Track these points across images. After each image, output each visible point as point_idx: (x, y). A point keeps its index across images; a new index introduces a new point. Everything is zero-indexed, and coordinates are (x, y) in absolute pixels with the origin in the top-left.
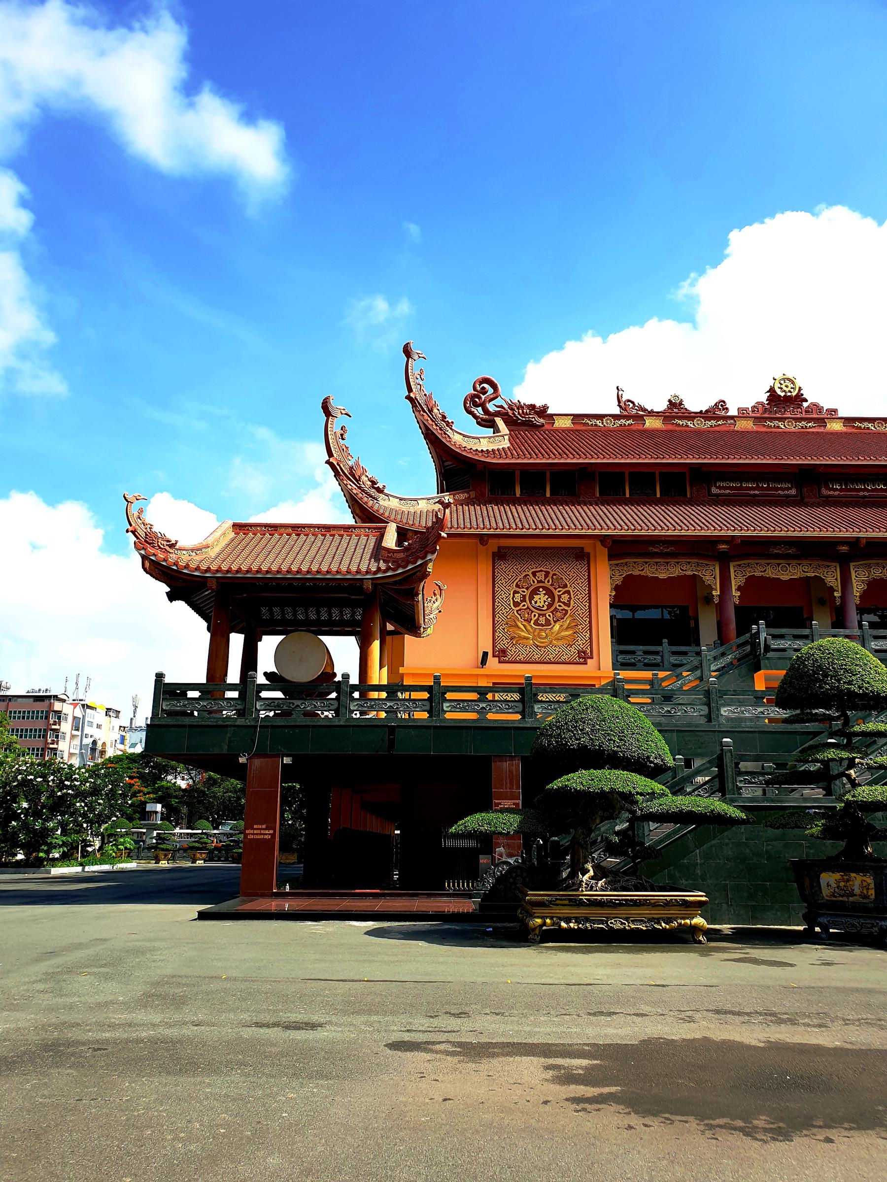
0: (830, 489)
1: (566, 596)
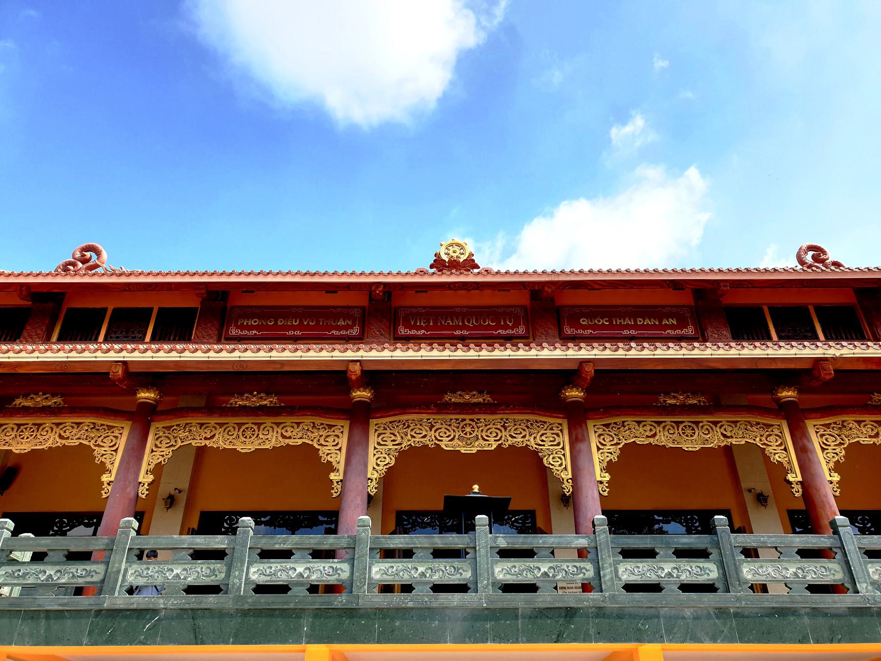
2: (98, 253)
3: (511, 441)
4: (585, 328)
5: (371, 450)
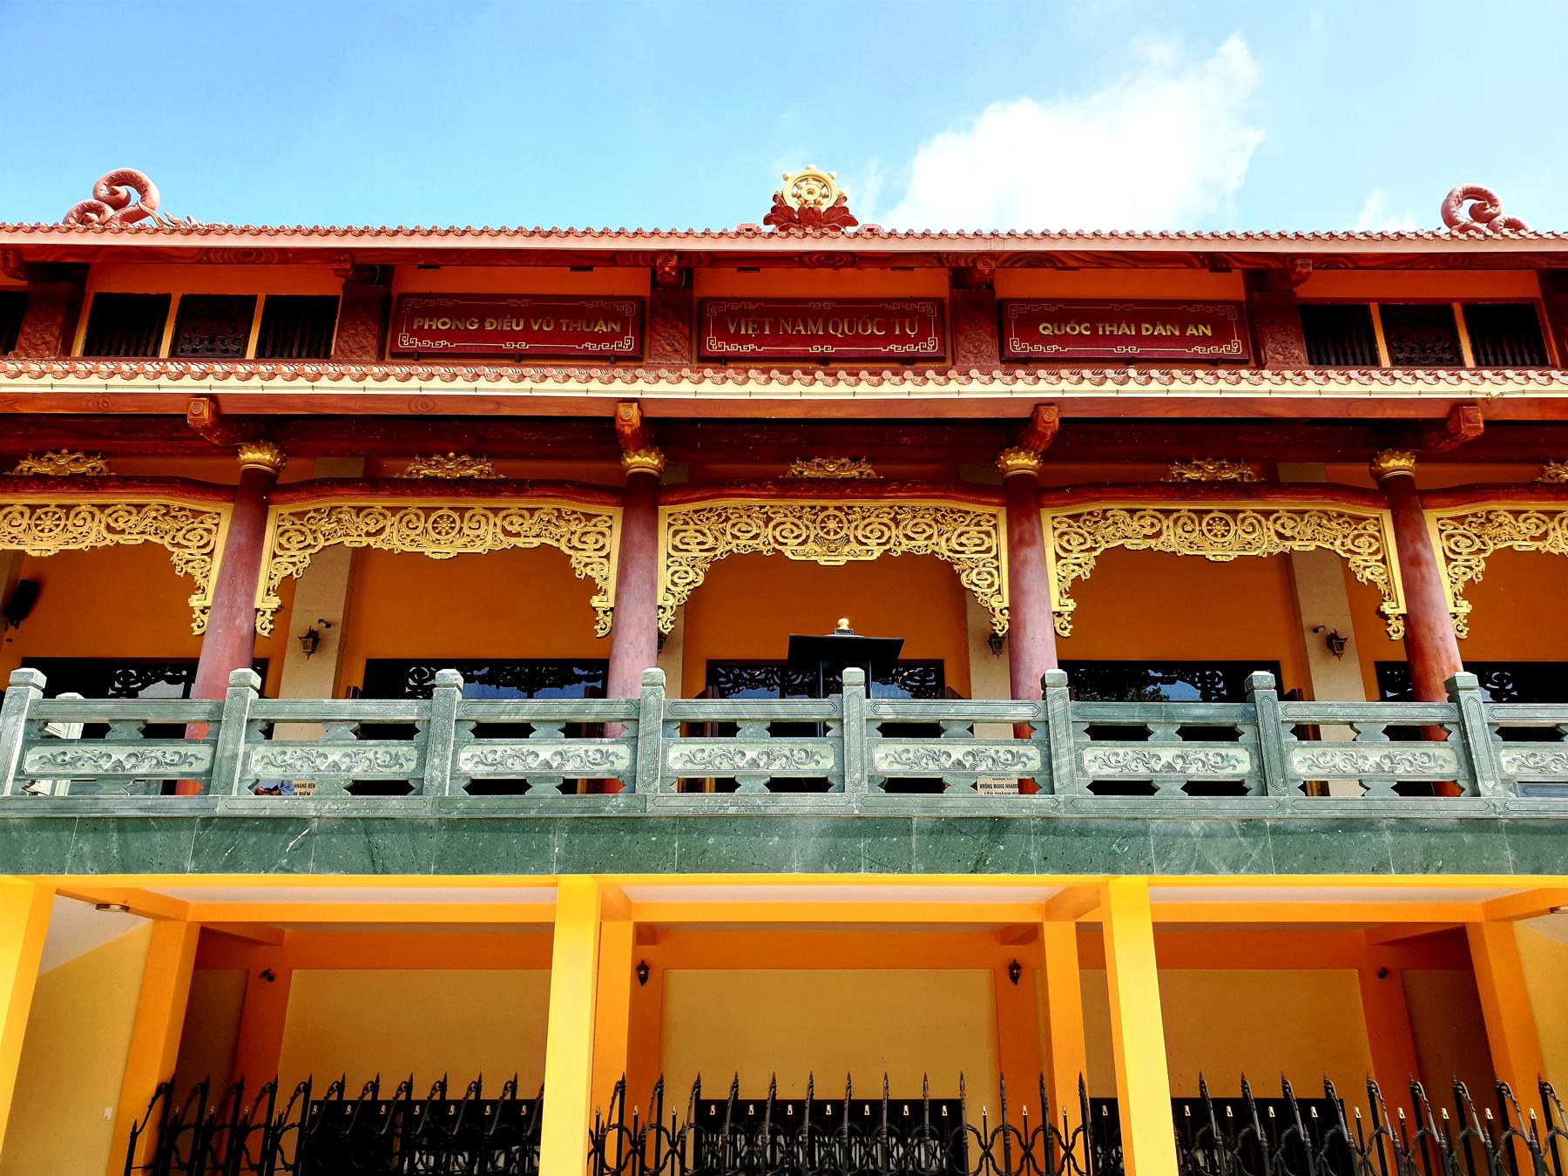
2: (142, 188)
3: (906, 545)
4: (1047, 341)
5: (662, 559)
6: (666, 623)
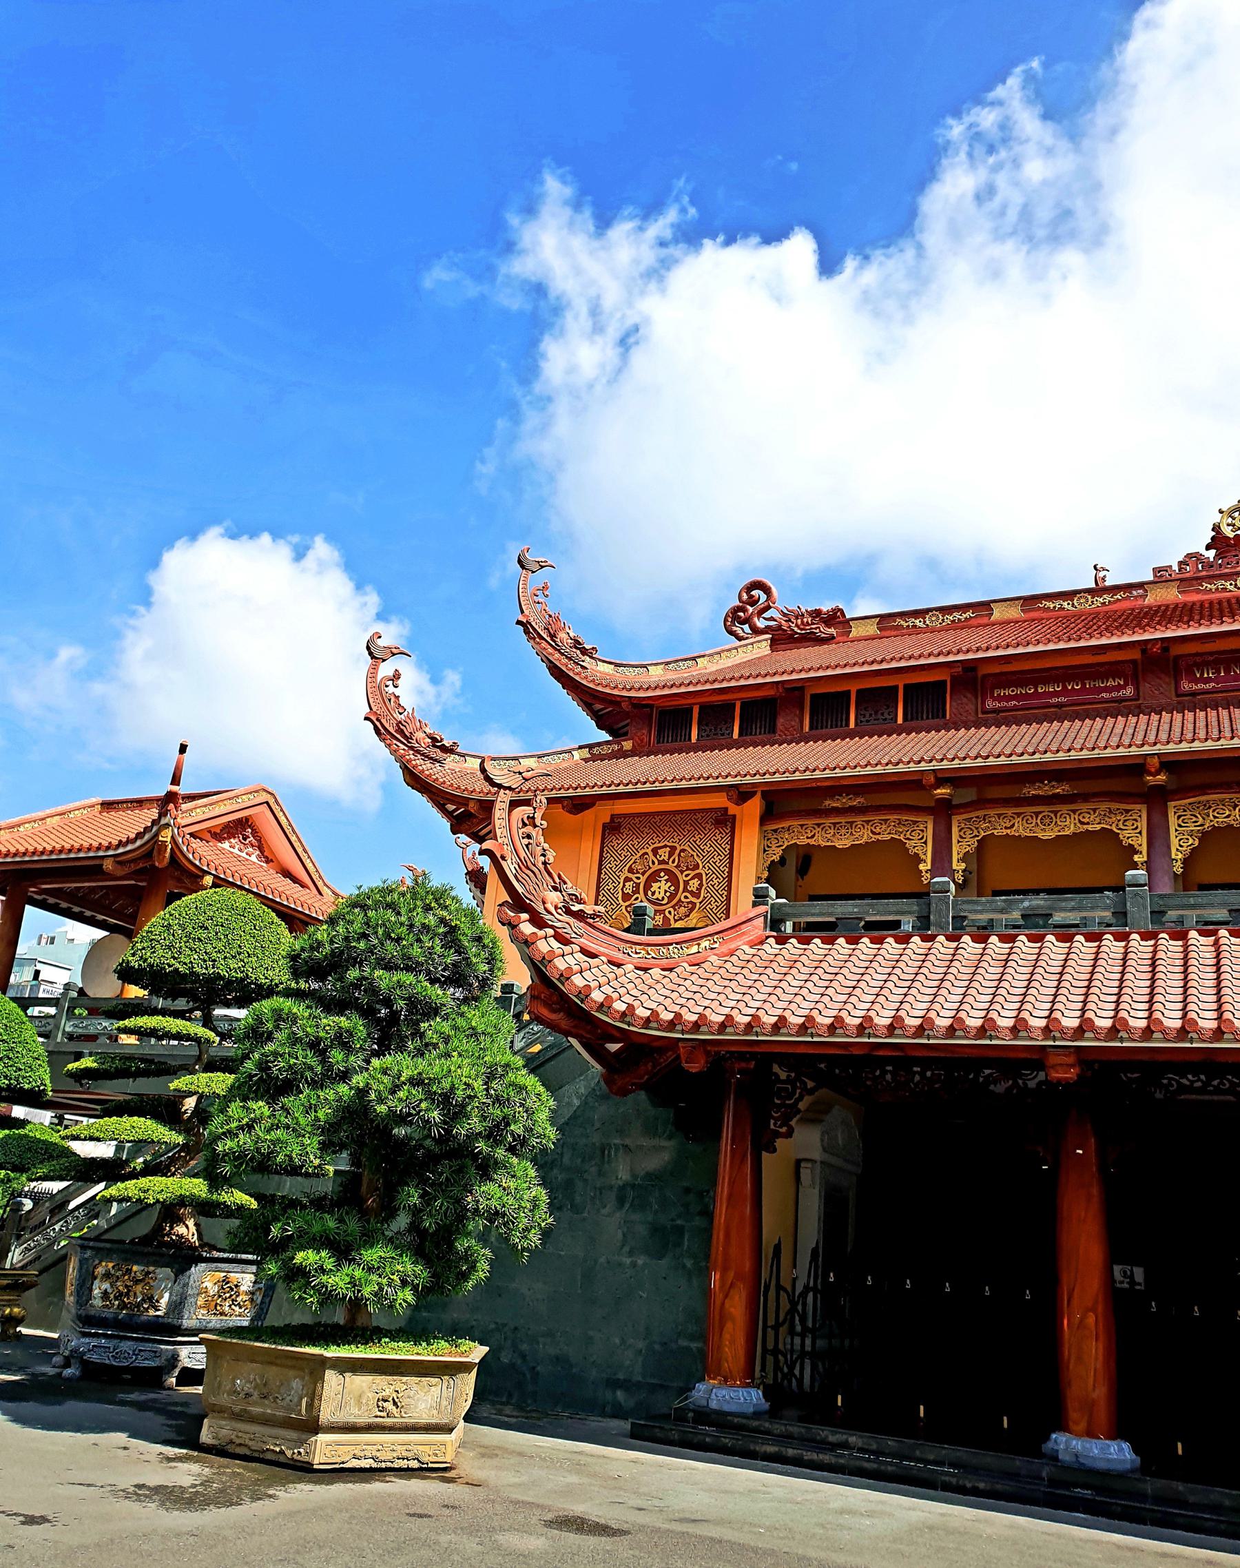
0: (1197, 681)
1: (696, 882)
2: (767, 590)
5: (1173, 833)
6: (1178, 868)
